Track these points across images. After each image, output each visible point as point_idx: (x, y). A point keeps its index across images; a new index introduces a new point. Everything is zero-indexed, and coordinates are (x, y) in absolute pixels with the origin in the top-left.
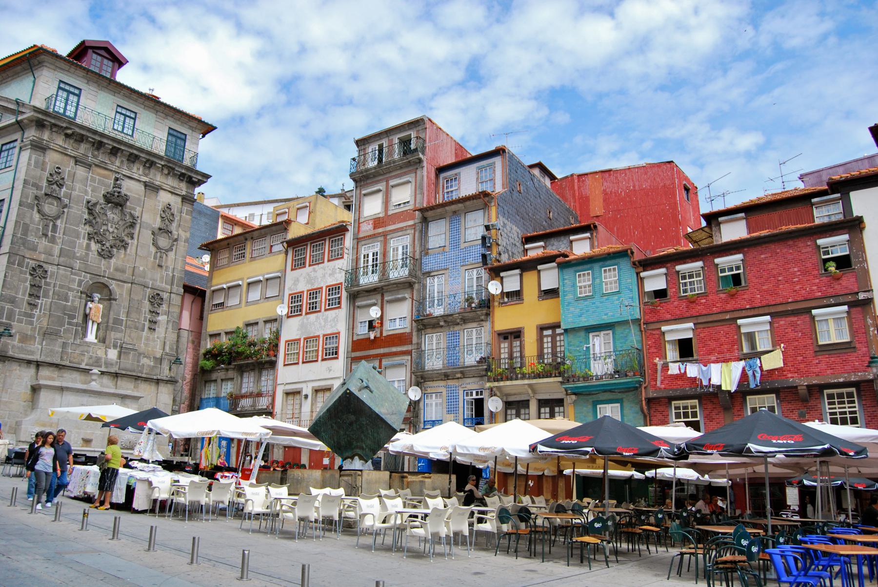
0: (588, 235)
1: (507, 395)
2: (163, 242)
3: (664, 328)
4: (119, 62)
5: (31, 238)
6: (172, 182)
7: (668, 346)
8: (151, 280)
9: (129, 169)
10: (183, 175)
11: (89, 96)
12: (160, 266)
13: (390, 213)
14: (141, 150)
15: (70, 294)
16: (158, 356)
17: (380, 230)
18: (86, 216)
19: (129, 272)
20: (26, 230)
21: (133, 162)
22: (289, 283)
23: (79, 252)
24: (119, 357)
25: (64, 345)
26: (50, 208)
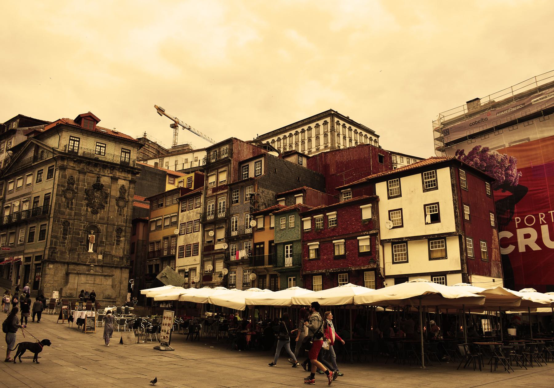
0: (302, 194)
1: (259, 272)
2: (121, 203)
3: (308, 244)
4: (97, 121)
5: (62, 209)
6: (123, 175)
7: (311, 252)
8: (117, 221)
9: (104, 172)
10: (128, 170)
11: (84, 141)
12: (120, 215)
13: (219, 185)
14: (108, 162)
15: (80, 232)
16: (121, 256)
17: (215, 194)
18: (85, 196)
19: (106, 219)
20: (60, 204)
21: (105, 168)
22: (180, 218)
23: (83, 213)
24: (103, 258)
25: (79, 255)
26: (69, 195)
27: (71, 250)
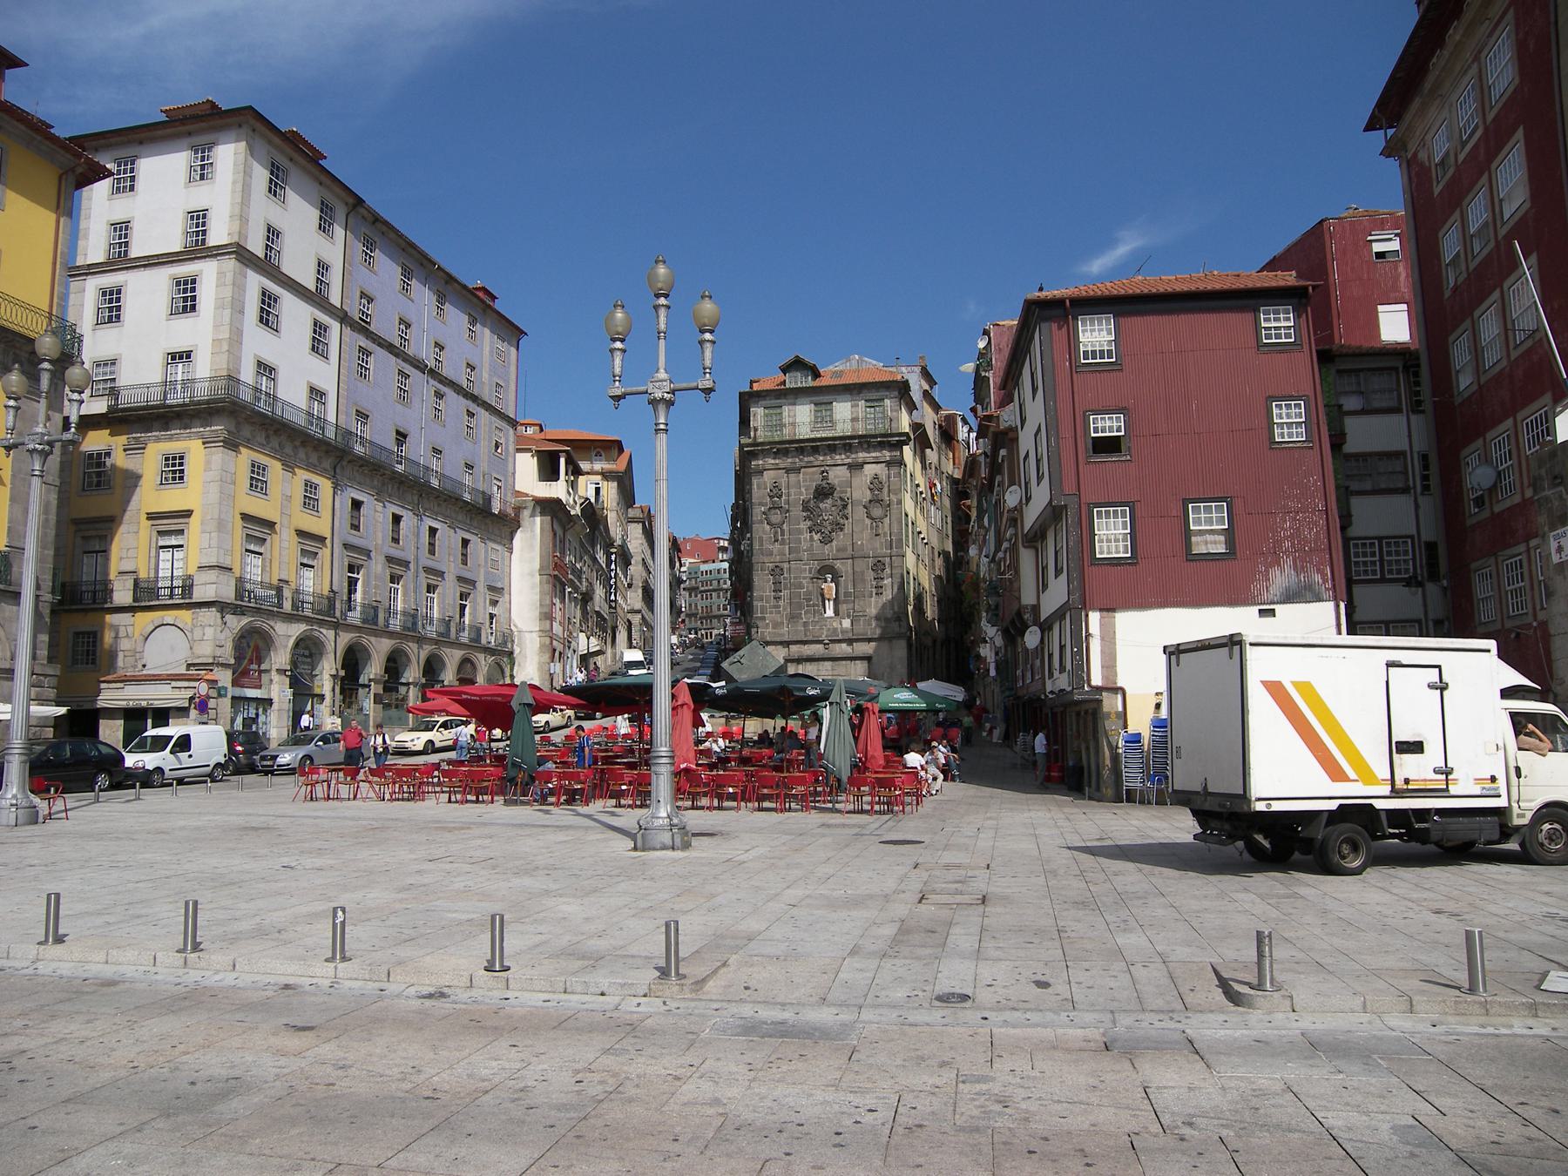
2: (877, 512)
23: (804, 546)
25: (805, 624)
26: (776, 517)
27: (793, 617)
